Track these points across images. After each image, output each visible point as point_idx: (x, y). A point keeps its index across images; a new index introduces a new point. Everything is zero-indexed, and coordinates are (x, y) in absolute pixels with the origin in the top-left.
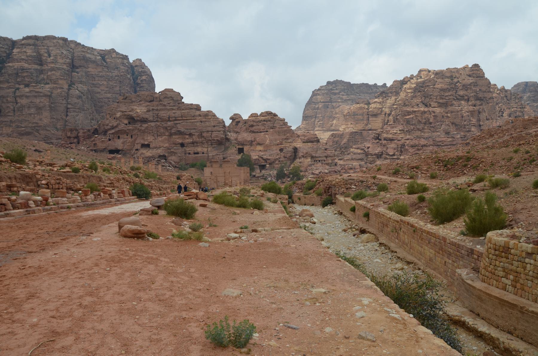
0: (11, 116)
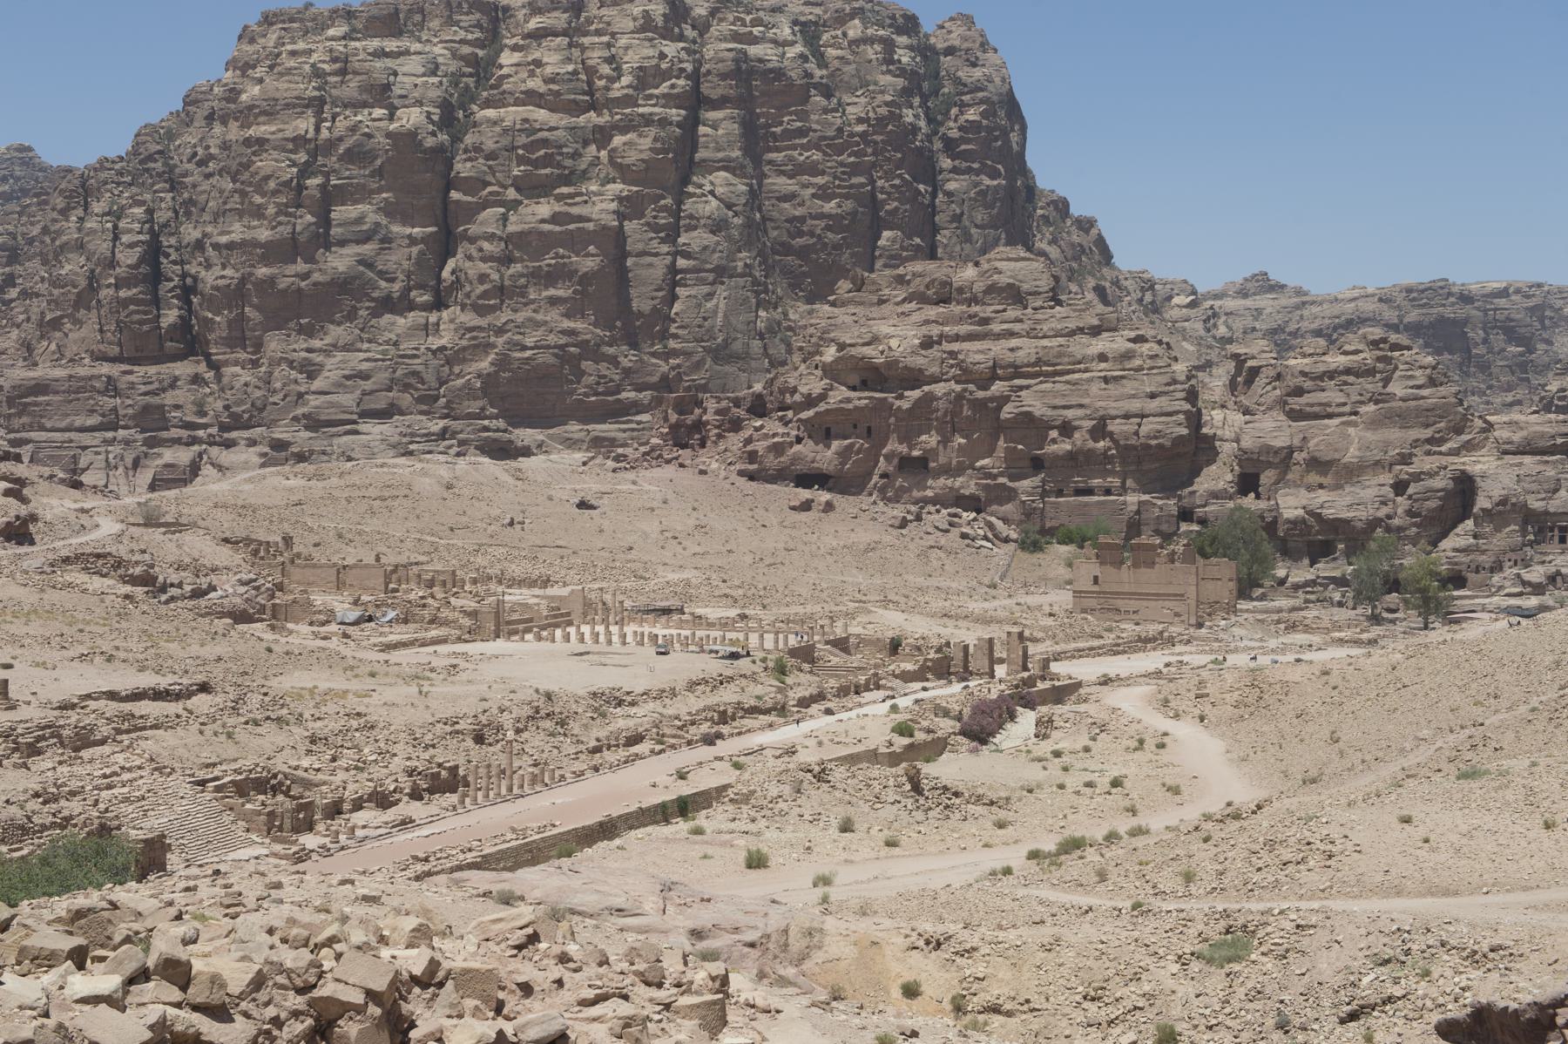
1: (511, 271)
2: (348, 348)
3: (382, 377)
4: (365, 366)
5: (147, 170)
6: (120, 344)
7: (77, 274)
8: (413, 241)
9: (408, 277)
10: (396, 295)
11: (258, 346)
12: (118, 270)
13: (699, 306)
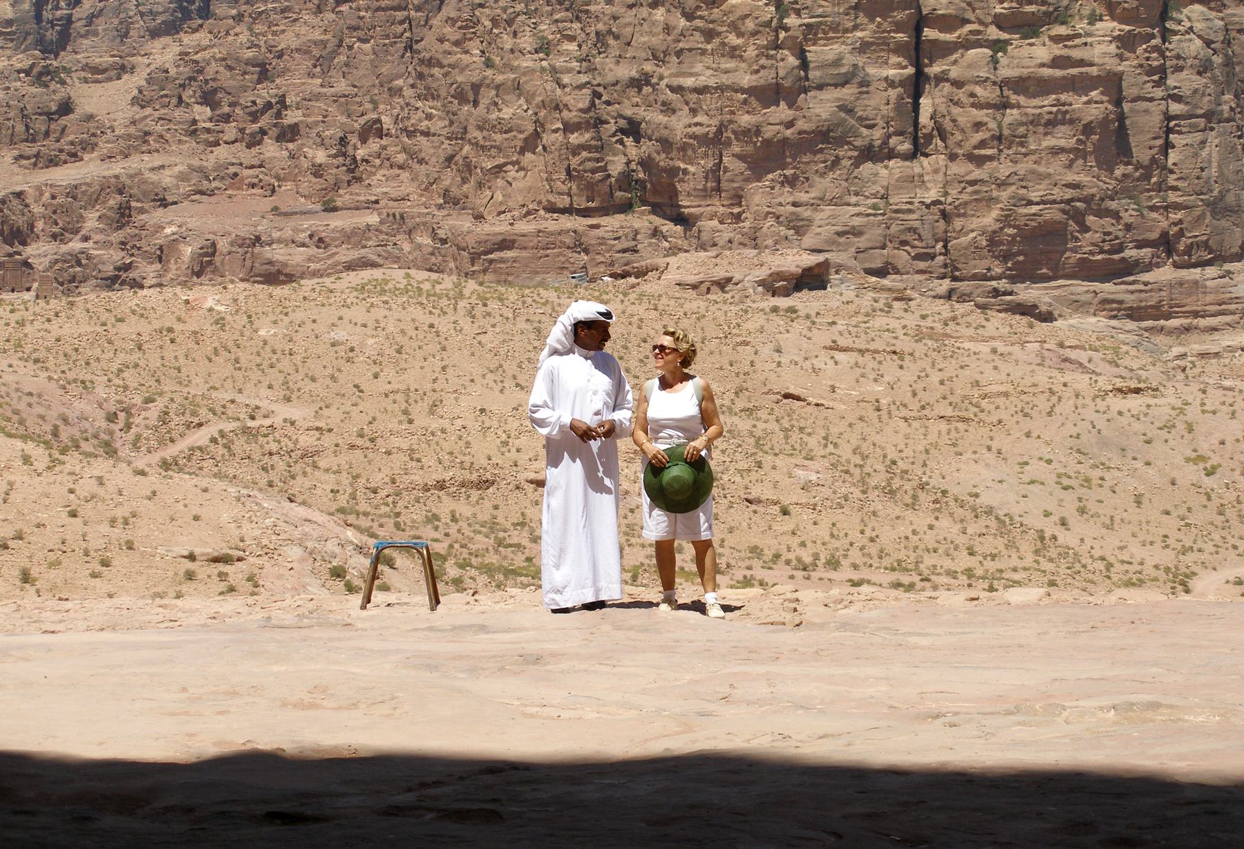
0: (990, 158)
1: (1008, 120)
2: (833, 202)
3: (875, 234)
4: (857, 221)
6: (569, 195)
7: (522, 118)
8: (891, 83)
9: (887, 123)
11: (738, 198)
12: (565, 113)
13: (1196, 155)
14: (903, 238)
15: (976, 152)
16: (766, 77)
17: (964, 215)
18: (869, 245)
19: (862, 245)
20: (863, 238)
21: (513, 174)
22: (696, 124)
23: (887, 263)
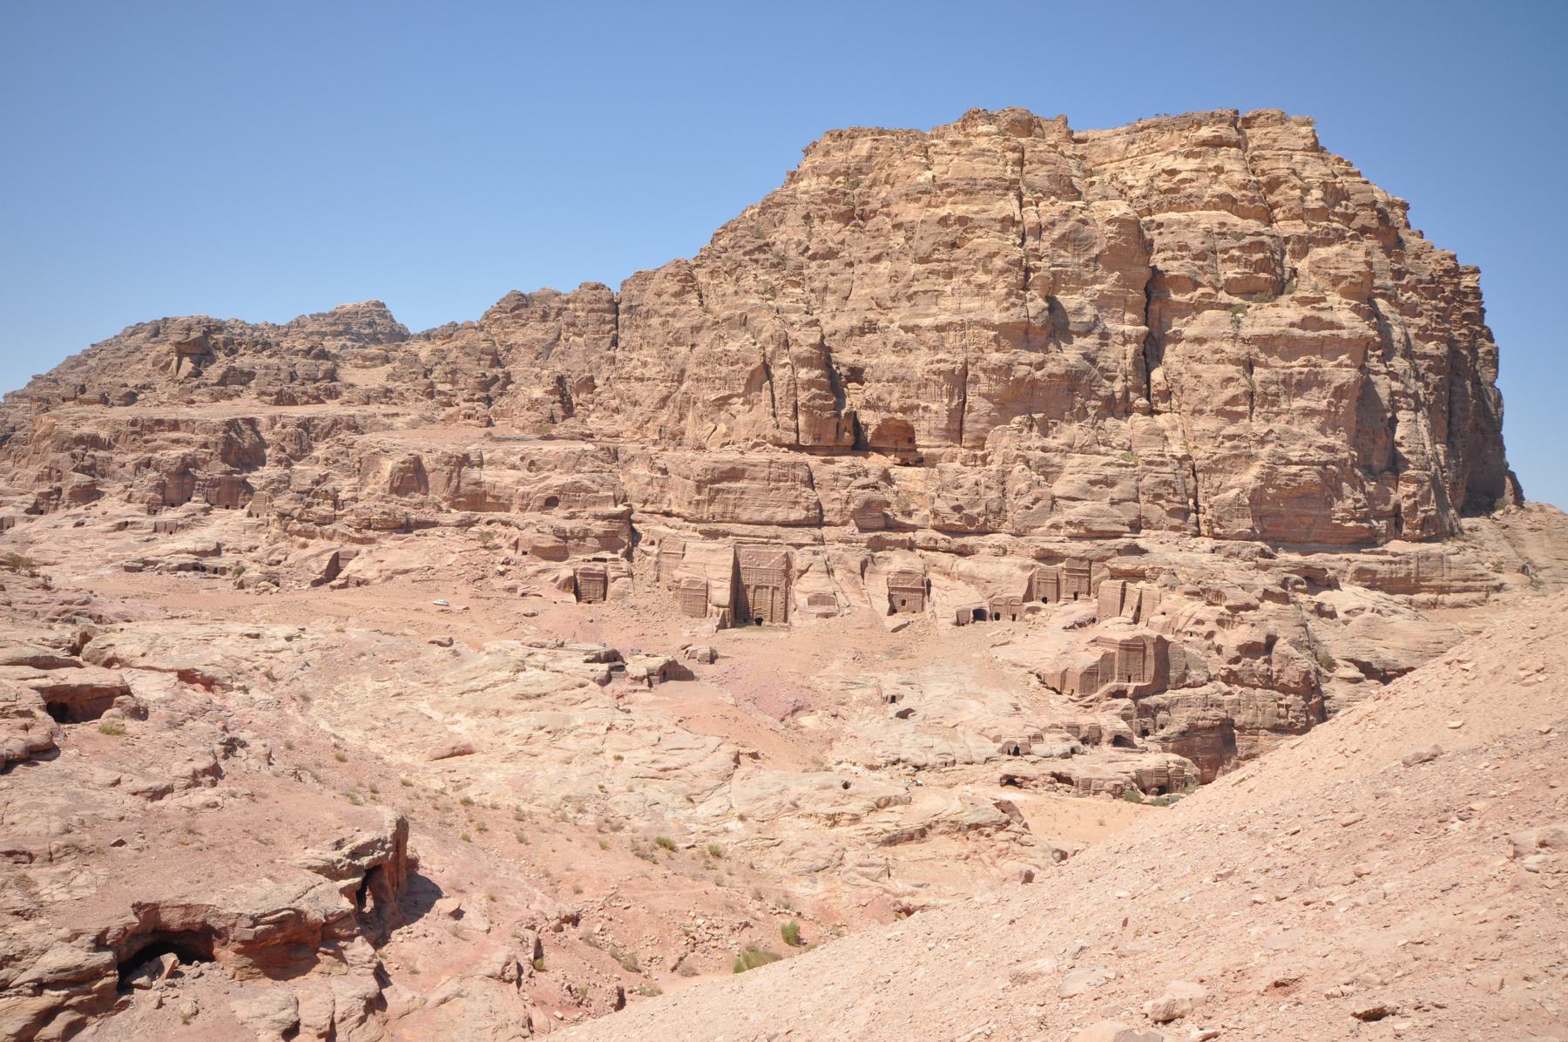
0: (1241, 415)
2: (1083, 450)
4: (1109, 471)
5: (756, 261)
10: (1118, 395)
11: (980, 442)
12: (794, 349)
14: (1158, 491)
15: (1228, 408)
16: (1015, 315)
17: (1221, 471)
18: (1123, 496)
19: (1116, 496)
20: (1116, 489)
21: (738, 407)
22: (939, 361)
23: (1140, 517)
